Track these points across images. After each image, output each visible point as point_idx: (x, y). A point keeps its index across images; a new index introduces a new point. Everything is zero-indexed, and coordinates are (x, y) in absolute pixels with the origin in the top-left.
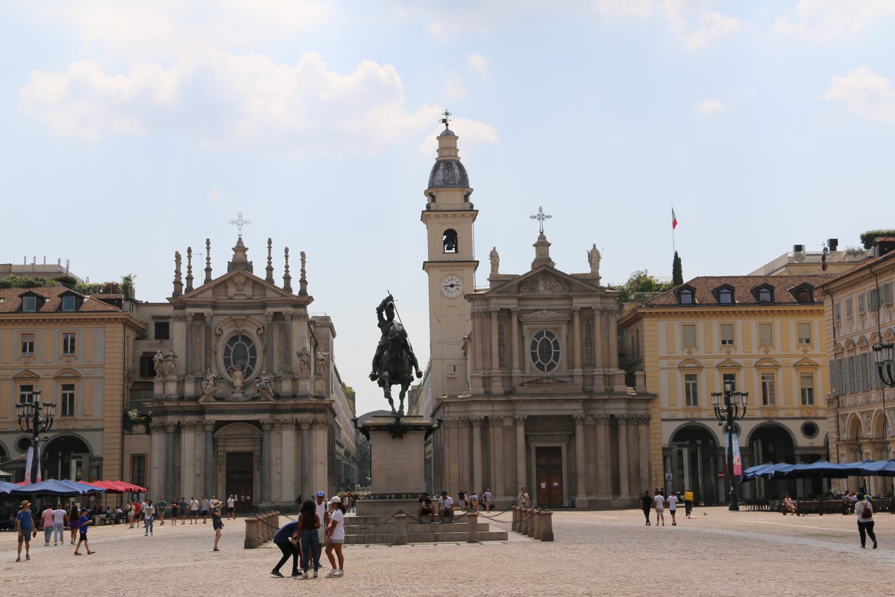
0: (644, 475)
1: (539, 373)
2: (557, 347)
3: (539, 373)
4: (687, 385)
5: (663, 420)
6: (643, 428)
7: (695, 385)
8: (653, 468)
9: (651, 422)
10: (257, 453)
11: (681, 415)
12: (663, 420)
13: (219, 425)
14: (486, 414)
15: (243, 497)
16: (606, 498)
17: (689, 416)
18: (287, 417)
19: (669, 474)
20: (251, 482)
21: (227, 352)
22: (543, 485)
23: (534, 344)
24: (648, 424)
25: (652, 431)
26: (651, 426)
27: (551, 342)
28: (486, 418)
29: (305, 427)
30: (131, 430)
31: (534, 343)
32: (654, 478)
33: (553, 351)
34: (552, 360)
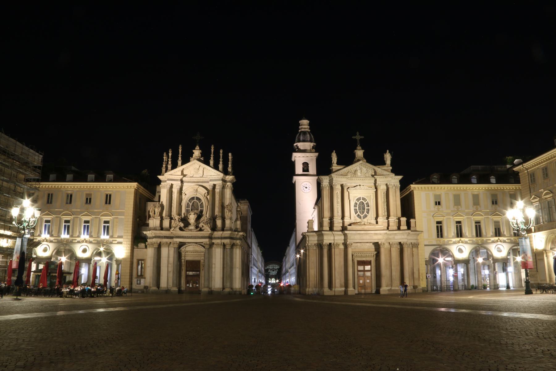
0: (416, 276)
1: (358, 220)
2: (368, 206)
3: (358, 220)
4: (437, 227)
5: (425, 245)
6: (414, 249)
7: (441, 227)
8: (421, 272)
9: (419, 246)
10: (202, 261)
11: (435, 243)
12: (425, 245)
13: (181, 245)
14: (330, 242)
15: (194, 285)
16: (397, 288)
17: (439, 243)
18: (219, 241)
19: (429, 275)
20: (198, 276)
21: (188, 206)
22: (361, 282)
23: (355, 206)
24: (417, 247)
25: (420, 251)
26: (419, 249)
27: (365, 203)
28: (330, 244)
29: (228, 247)
30: (138, 246)
31: (356, 204)
32: (421, 277)
33: (366, 208)
34: (365, 213)
